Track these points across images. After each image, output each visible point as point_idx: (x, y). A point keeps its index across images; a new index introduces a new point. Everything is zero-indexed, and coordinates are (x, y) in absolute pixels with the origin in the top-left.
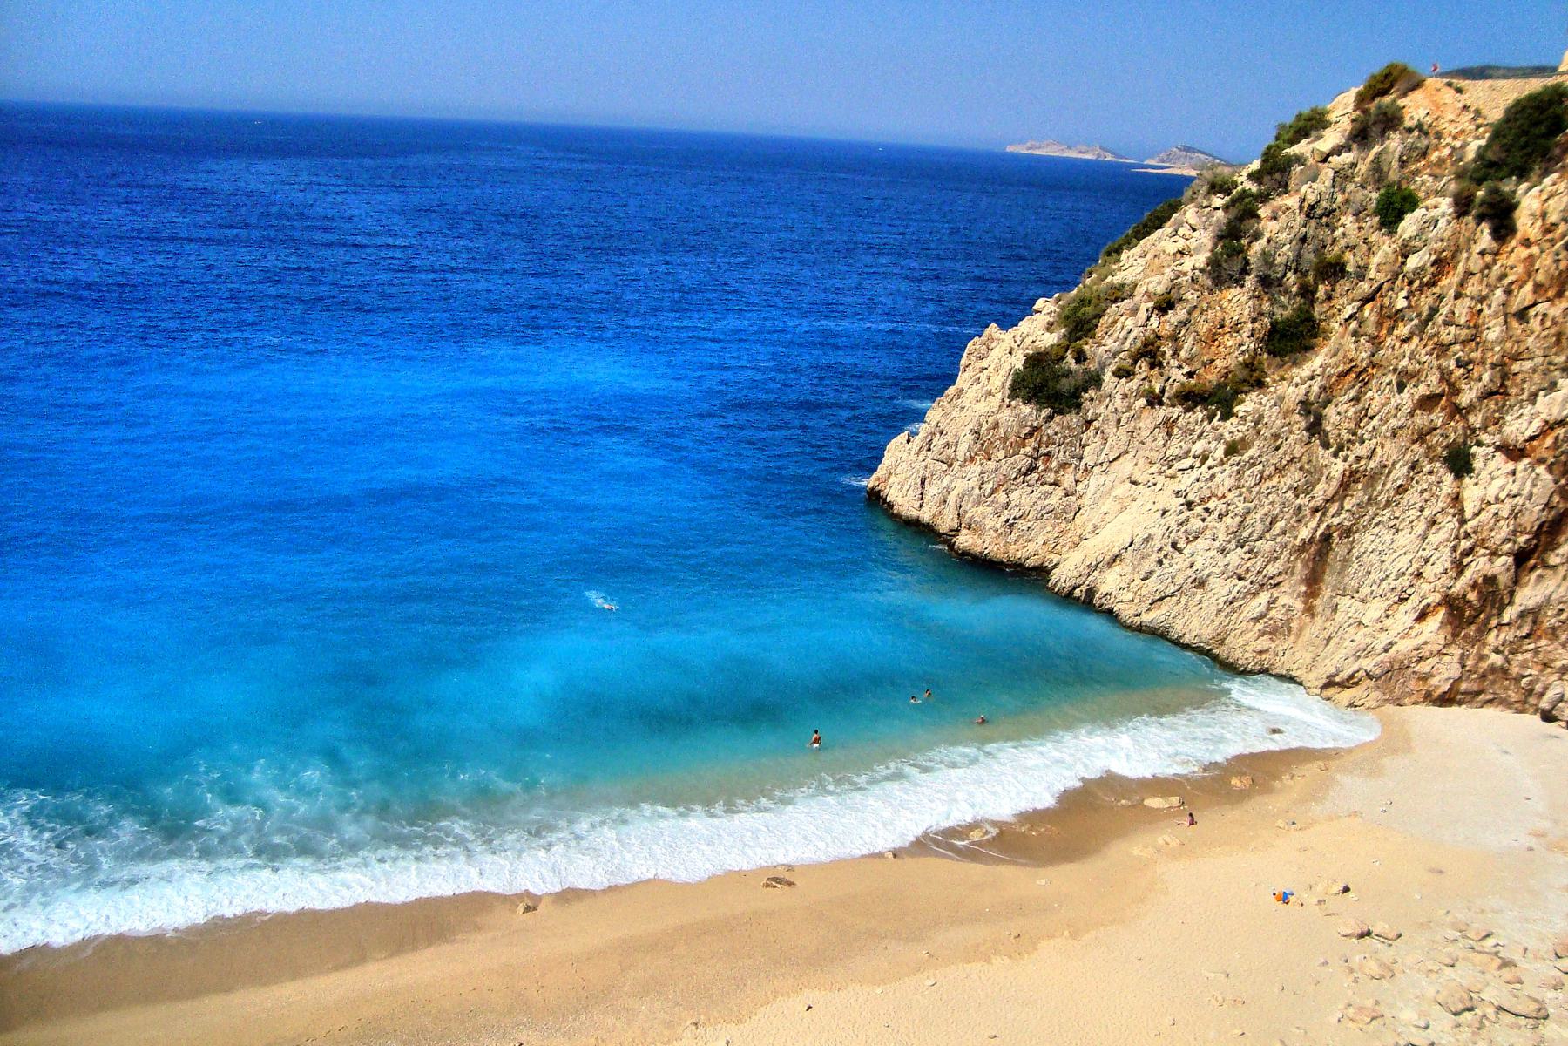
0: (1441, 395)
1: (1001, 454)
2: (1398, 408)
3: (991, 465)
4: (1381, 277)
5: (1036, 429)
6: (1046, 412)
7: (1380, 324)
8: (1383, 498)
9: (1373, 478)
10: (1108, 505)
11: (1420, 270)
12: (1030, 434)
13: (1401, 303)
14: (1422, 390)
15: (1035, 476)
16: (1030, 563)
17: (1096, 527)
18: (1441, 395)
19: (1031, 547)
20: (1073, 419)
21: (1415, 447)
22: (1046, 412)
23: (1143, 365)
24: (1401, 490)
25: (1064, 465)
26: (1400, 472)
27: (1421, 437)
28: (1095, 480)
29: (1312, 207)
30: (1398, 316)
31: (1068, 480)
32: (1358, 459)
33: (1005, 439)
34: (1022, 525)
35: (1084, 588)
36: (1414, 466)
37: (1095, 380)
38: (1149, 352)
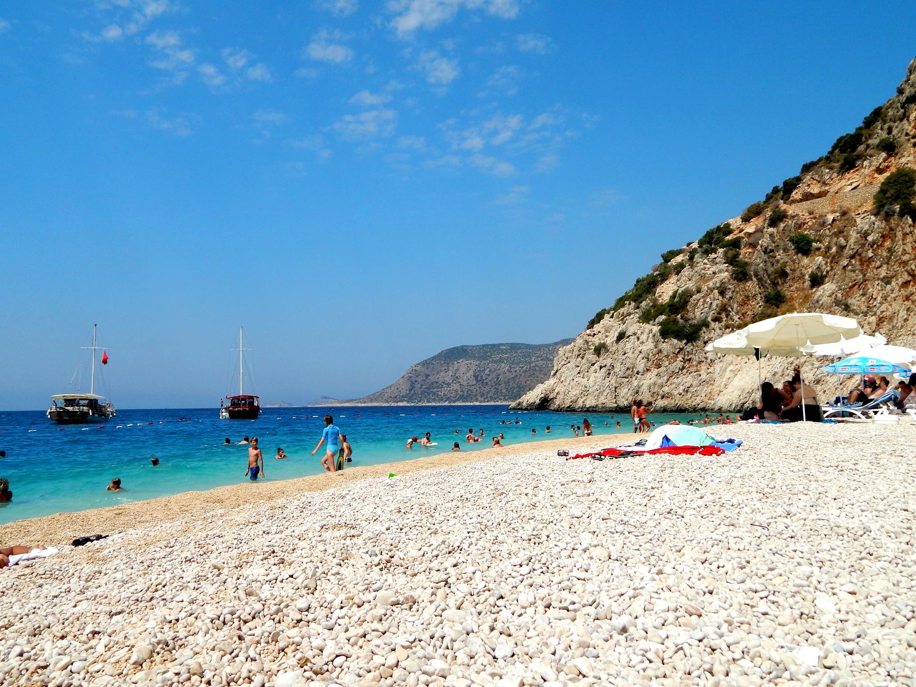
0: (910, 281)
1: (667, 363)
2: (892, 291)
3: (662, 369)
4: (857, 247)
5: (681, 349)
6: (684, 341)
7: (862, 264)
8: (899, 325)
9: (891, 319)
10: (728, 374)
11: (874, 243)
12: (679, 352)
13: (870, 254)
14: (900, 281)
15: (685, 371)
16: (701, 406)
17: (726, 385)
18: (910, 281)
19: (698, 400)
20: (700, 343)
21: (906, 303)
22: (684, 341)
23: (723, 315)
24: (906, 320)
25: (700, 362)
26: (903, 314)
27: (907, 298)
28: (718, 367)
29: (766, 249)
30: (870, 260)
31: (703, 367)
32: (882, 312)
33: (667, 356)
34: (691, 389)
35: (750, 402)
36: (908, 309)
37: (707, 325)
38: (724, 309)
